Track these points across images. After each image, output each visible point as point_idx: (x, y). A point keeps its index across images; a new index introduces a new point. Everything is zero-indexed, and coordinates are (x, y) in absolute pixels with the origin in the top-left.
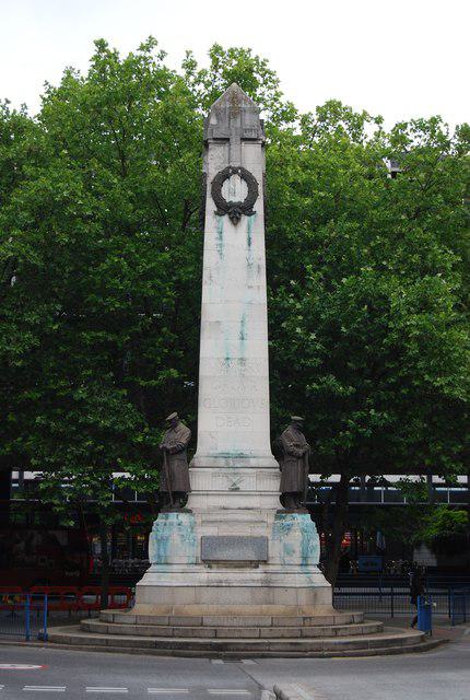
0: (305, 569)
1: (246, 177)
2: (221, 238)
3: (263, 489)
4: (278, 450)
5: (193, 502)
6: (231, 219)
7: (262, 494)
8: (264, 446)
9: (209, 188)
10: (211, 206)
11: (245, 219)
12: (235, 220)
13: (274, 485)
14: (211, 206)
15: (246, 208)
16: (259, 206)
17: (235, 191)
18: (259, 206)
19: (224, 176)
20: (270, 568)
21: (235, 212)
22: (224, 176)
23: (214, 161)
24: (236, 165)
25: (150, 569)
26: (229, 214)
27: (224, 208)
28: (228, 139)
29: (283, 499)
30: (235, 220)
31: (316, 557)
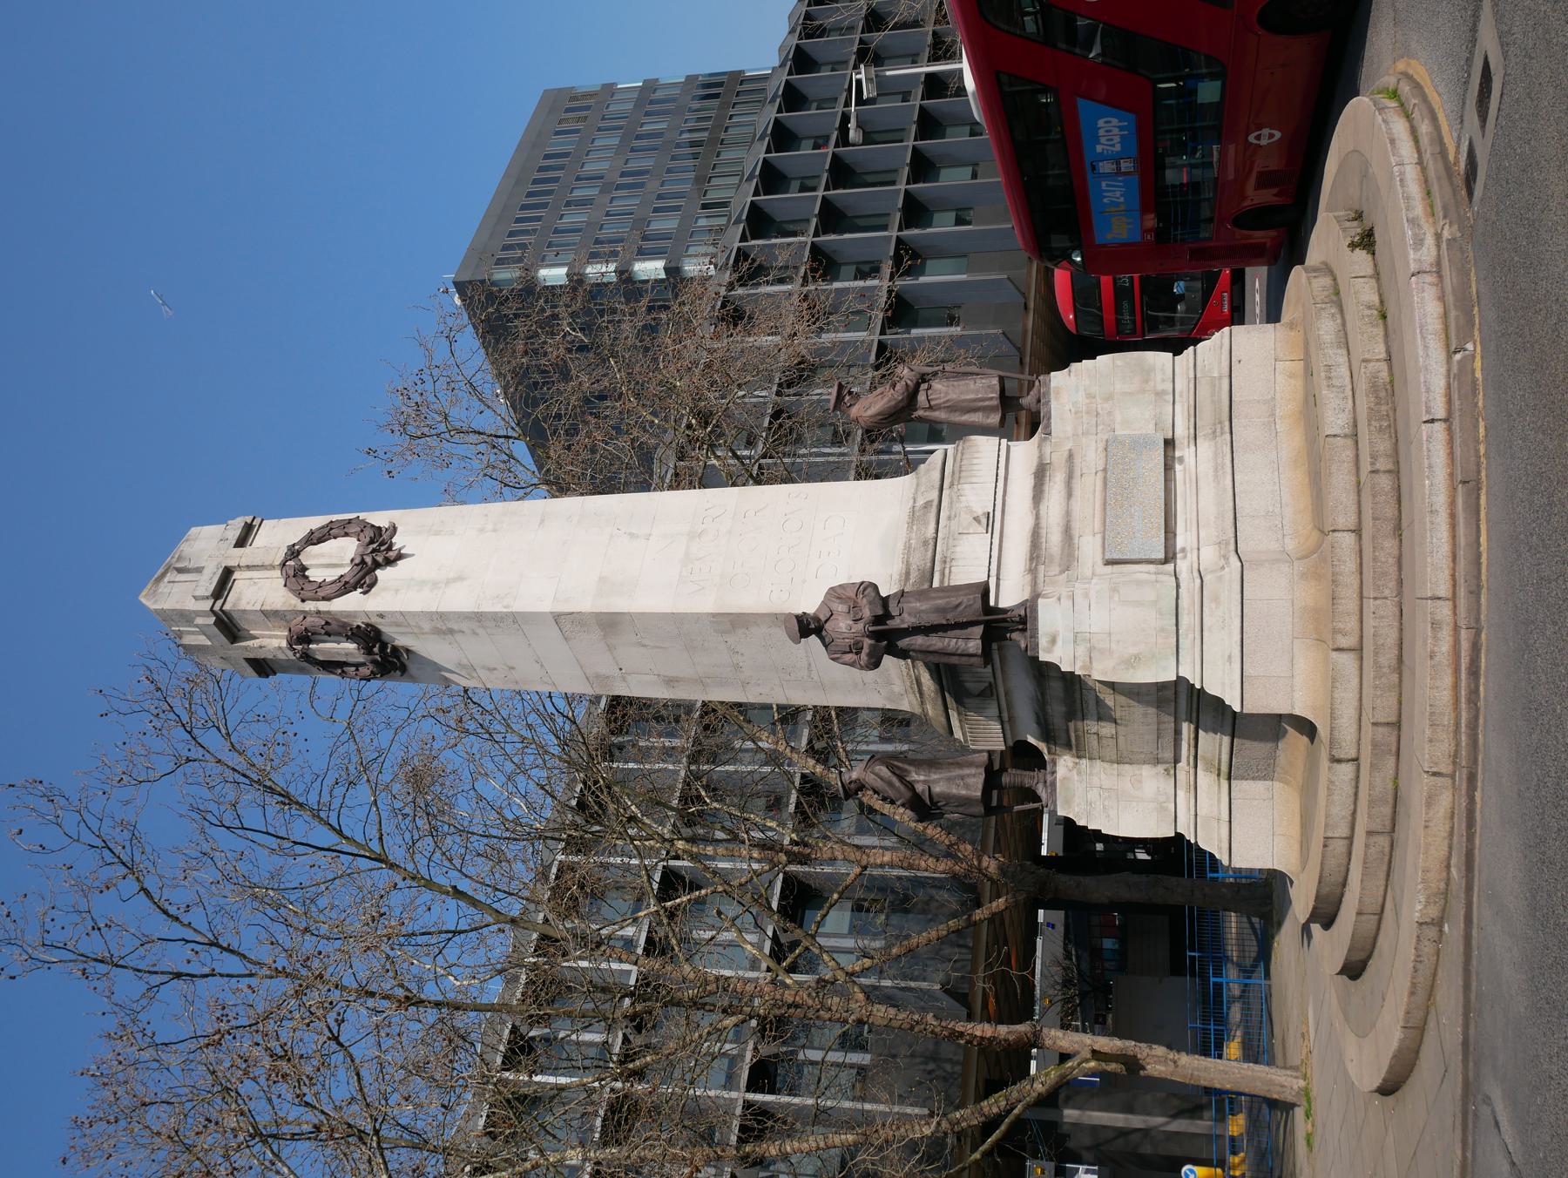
1: (315, 538)
2: (423, 583)
3: (988, 466)
5: (1009, 596)
6: (389, 562)
10: (352, 604)
11: (398, 541)
14: (352, 604)
16: (380, 519)
20: (1182, 431)
21: (379, 552)
22: (296, 574)
25: (1191, 838)
26: (377, 565)
27: (363, 577)
28: (227, 573)
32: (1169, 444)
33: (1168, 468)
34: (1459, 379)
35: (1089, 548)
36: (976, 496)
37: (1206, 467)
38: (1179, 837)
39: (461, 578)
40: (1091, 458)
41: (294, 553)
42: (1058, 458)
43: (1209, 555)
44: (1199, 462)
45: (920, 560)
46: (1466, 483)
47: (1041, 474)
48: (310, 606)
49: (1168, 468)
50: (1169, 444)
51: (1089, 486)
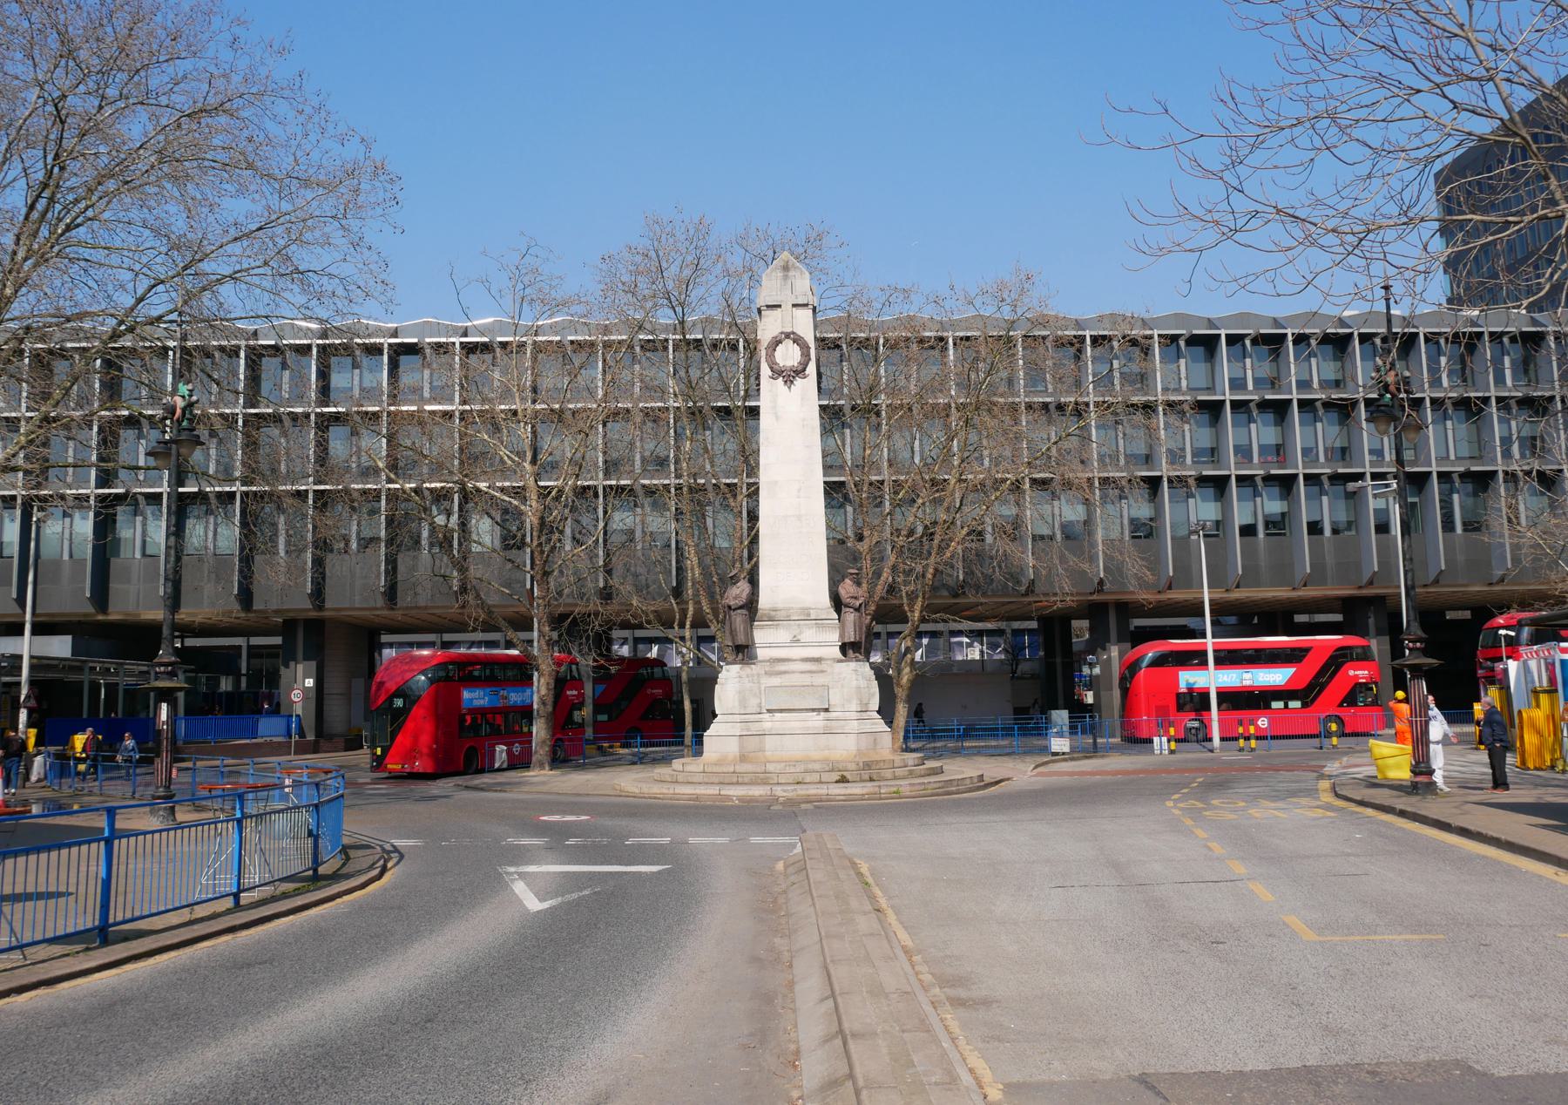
0: (865, 715)
1: (798, 340)
4: (838, 603)
7: (820, 645)
8: (825, 599)
9: (763, 353)
11: (798, 382)
12: (789, 381)
13: (834, 637)
14: (765, 371)
15: (800, 372)
17: (788, 355)
18: (812, 369)
19: (777, 342)
20: (832, 715)
21: (790, 376)
22: (777, 342)
23: (768, 328)
24: (789, 330)
27: (777, 372)
29: (844, 648)
30: (789, 381)
31: (875, 704)
32: (827, 710)
33: (813, 710)
34: (728, 797)
35: (776, 681)
36: (809, 634)
37: (810, 724)
38: (715, 716)
39: (777, 418)
40: (819, 680)
41: (788, 336)
42: (824, 666)
43: (767, 725)
44: (817, 721)
45: (781, 615)
46: (697, 798)
47: (818, 660)
48: (763, 353)
49: (813, 710)
50: (827, 710)
51: (807, 679)
